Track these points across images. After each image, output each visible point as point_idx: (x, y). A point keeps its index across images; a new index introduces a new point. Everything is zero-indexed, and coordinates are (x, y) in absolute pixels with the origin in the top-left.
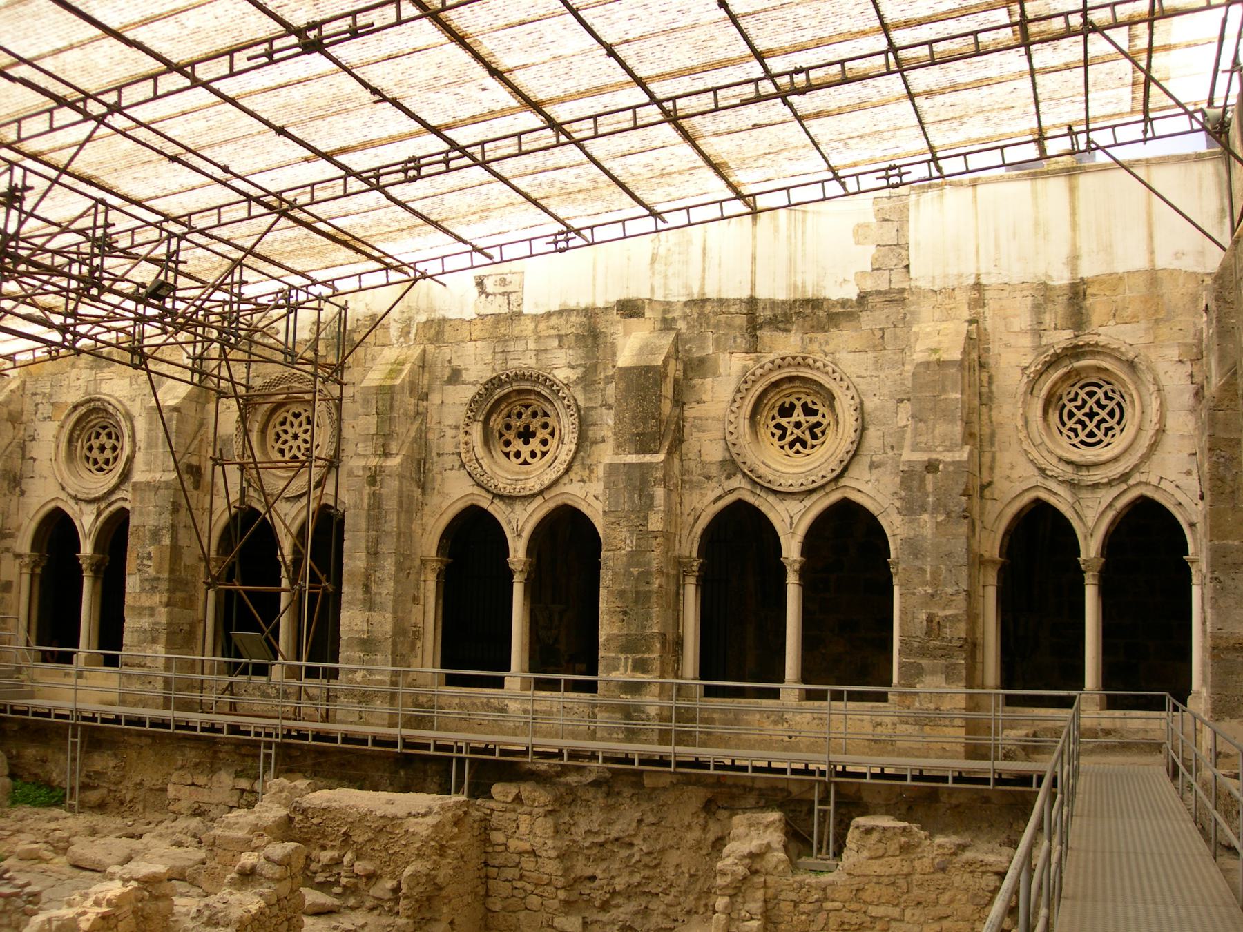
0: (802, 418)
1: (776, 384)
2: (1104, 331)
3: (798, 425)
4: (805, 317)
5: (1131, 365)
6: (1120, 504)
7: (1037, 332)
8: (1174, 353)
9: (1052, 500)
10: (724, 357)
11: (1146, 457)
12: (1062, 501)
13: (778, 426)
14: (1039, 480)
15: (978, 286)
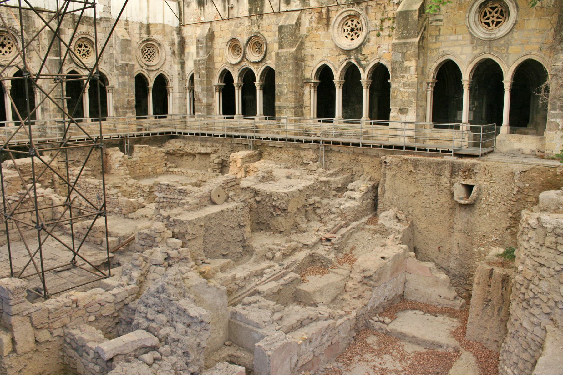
0: (85, 48)
1: (79, 39)
2: (154, 36)
3: (84, 50)
4: (87, 21)
5: (159, 45)
6: (157, 75)
7: (140, 34)
8: (167, 43)
9: (144, 73)
10: (67, 29)
11: (162, 65)
12: (146, 74)
13: (78, 50)
14: (141, 69)
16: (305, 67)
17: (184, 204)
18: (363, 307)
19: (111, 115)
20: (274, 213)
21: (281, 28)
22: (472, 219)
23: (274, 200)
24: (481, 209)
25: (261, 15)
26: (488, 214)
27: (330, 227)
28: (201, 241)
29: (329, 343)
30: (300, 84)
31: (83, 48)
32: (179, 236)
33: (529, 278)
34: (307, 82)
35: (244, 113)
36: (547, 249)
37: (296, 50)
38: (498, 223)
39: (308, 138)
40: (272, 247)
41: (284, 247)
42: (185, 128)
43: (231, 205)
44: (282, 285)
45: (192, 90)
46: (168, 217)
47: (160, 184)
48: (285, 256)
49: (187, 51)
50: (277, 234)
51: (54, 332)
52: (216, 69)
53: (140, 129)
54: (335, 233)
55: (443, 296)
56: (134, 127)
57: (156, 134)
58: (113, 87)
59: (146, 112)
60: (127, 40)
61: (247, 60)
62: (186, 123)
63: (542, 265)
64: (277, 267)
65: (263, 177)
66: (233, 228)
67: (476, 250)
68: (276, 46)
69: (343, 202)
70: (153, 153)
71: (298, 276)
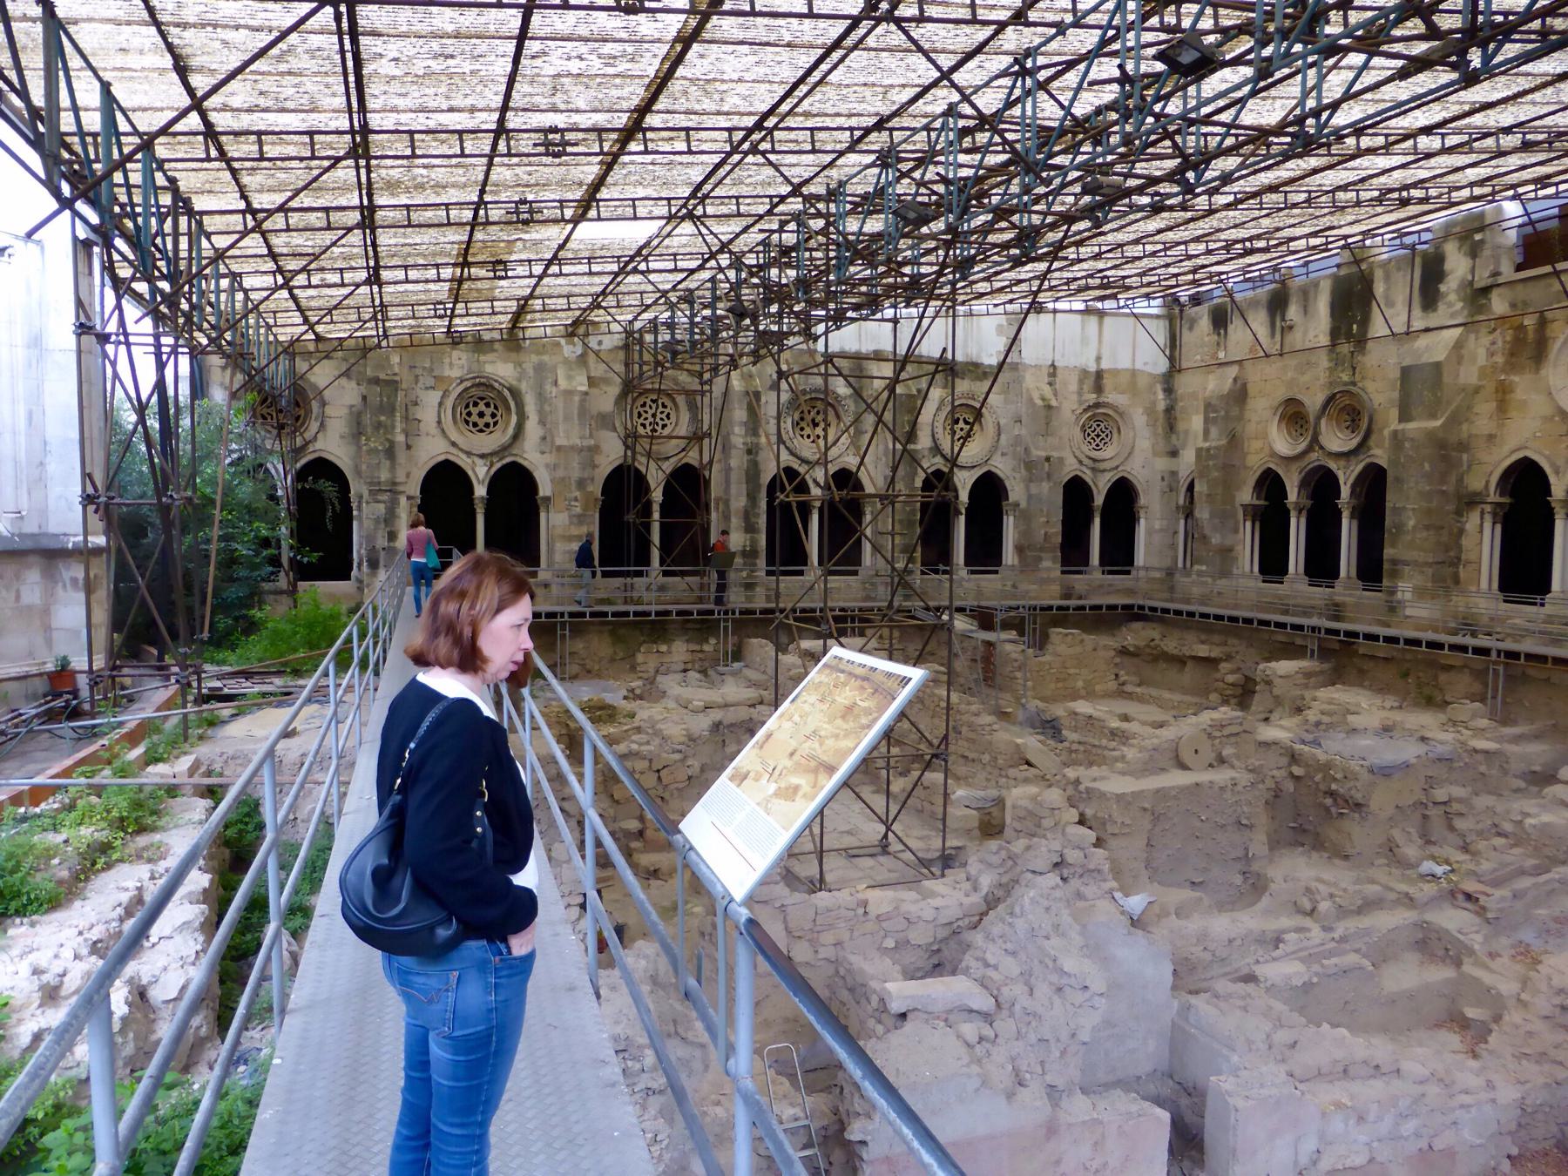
2: (1111, 397)
5: (1121, 414)
7: (1080, 393)
12: (1088, 476)
14: (1077, 466)
15: (1053, 365)
16: (1469, 467)
17: (1116, 760)
18: (1547, 1085)
19: (1010, 562)
20: (1333, 810)
21: (1406, 372)
23: (1335, 780)
25: (1361, 341)
27: (1485, 866)
28: (1141, 842)
29: (1423, 1144)
30: (1451, 507)
31: (961, 424)
32: (1093, 824)
34: (1471, 501)
35: (1308, 572)
37: (1443, 425)
39: (1469, 641)
40: (1313, 885)
41: (1345, 890)
42: (1172, 600)
43: (1221, 776)
44: (1317, 974)
45: (1189, 514)
46: (1077, 782)
47: (1076, 714)
48: (1343, 912)
49: (1181, 426)
50: (1337, 861)
51: (821, 950)
52: (1246, 468)
53: (1067, 596)
54: (1496, 883)
56: (1056, 589)
57: (1099, 607)
58: (1017, 505)
59: (1085, 561)
60: (1049, 407)
61: (1322, 448)
62: (1172, 589)
64: (1316, 934)
65: (1318, 724)
66: (1223, 826)
68: (1394, 413)
69: (1532, 810)
70: (1089, 647)
71: (1367, 963)
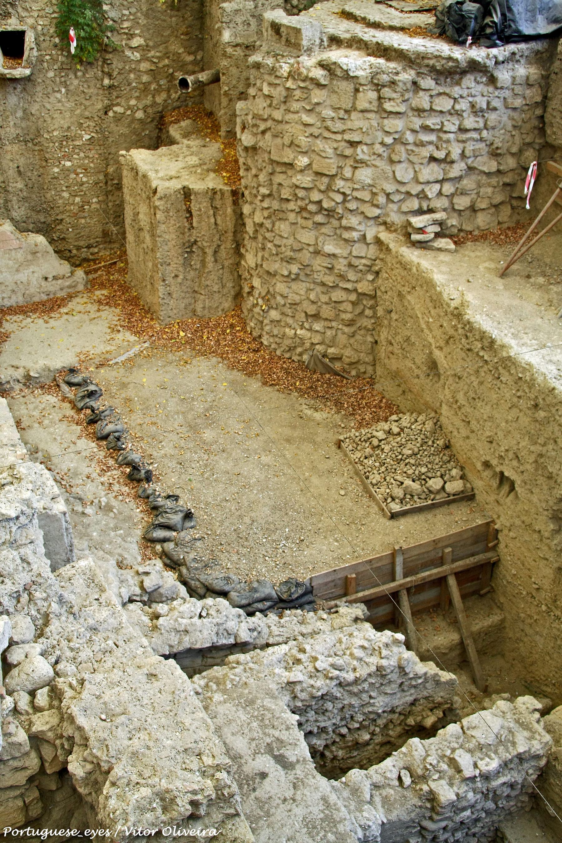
22: (34, 108)
24: (48, 82)
26: (63, 90)
33: (333, 172)
36: (360, 115)
38: (87, 103)
55: (50, 276)
63: (353, 144)
67: (56, 170)
